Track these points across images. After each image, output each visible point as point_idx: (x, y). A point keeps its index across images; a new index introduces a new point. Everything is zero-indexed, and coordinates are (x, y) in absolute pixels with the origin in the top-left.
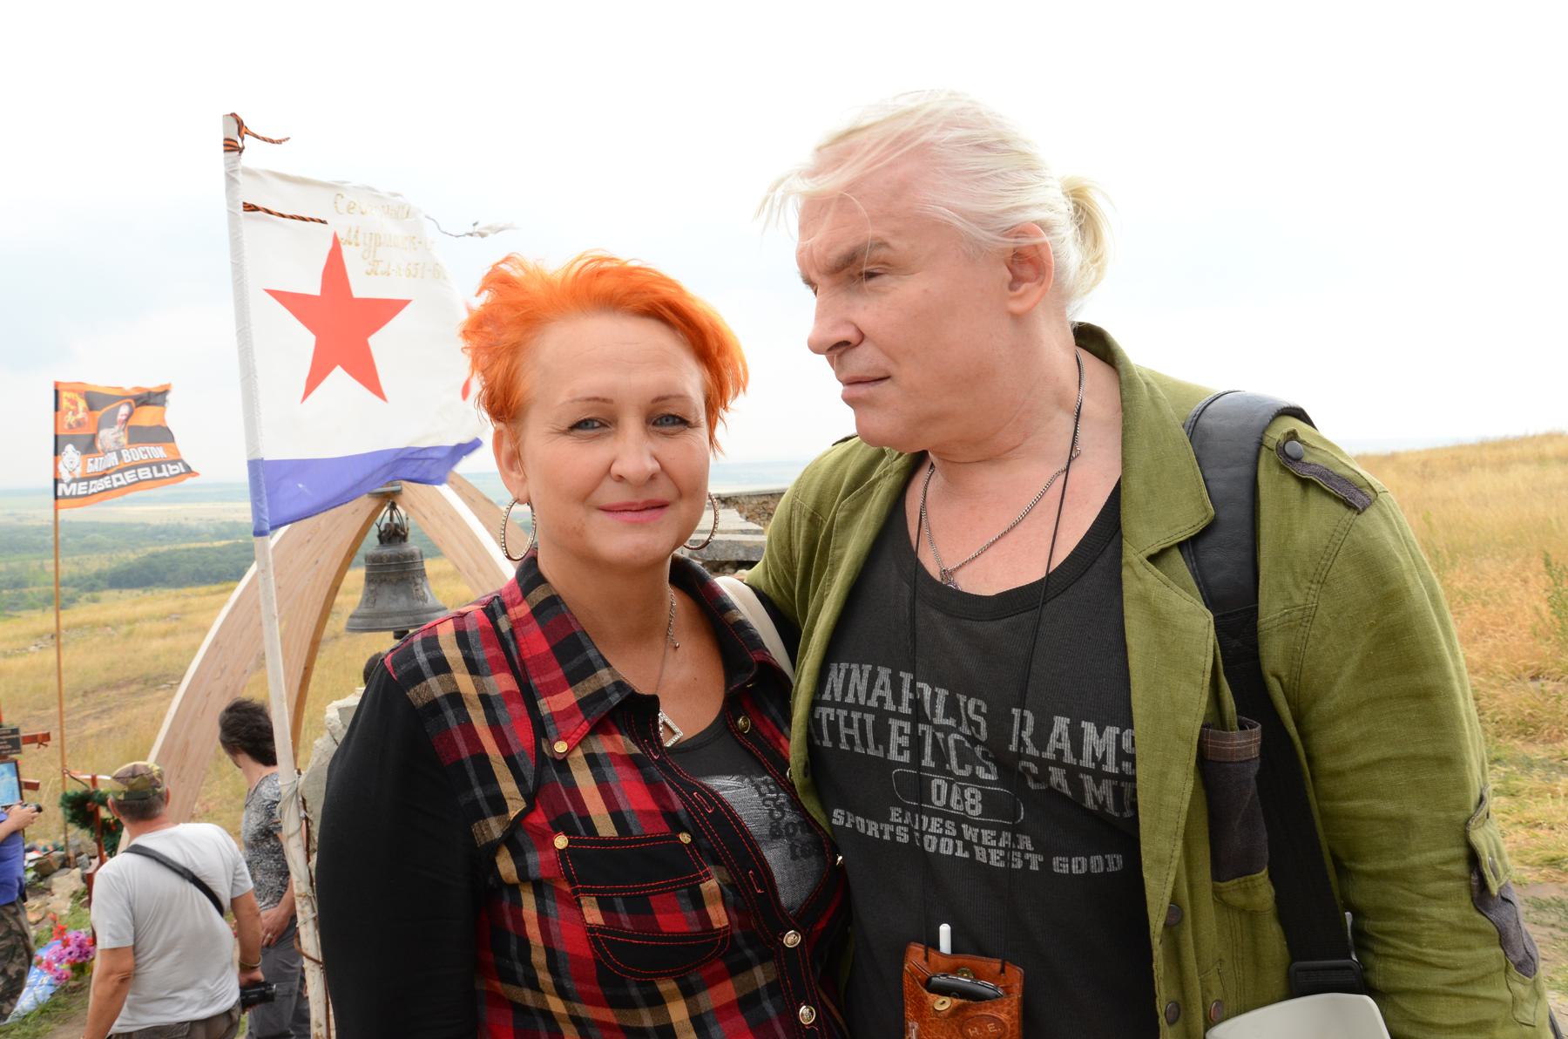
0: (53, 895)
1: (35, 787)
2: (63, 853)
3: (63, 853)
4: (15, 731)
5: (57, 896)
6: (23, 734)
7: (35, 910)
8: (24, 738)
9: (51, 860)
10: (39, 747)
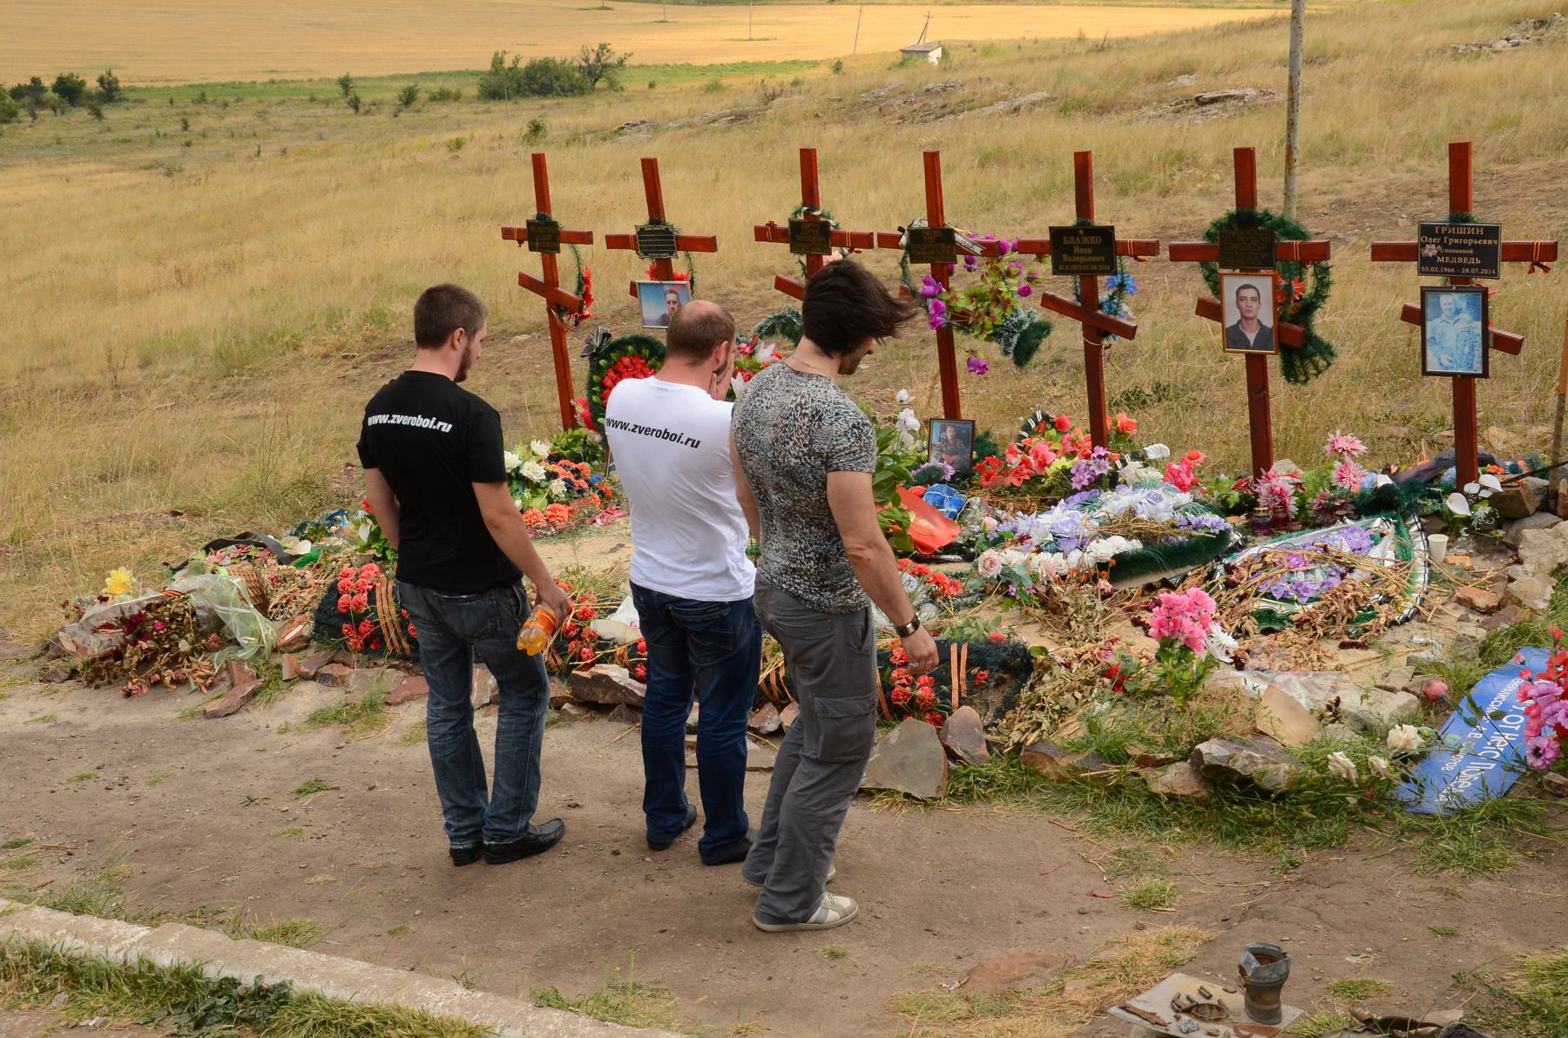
0: (1519, 562)
1: (1511, 347)
2: (1546, 482)
3: (1546, 482)
4: (1493, 232)
5: (1528, 567)
6: (1507, 237)
7: (1485, 584)
8: (1506, 246)
9: (1524, 493)
10: (1532, 271)
